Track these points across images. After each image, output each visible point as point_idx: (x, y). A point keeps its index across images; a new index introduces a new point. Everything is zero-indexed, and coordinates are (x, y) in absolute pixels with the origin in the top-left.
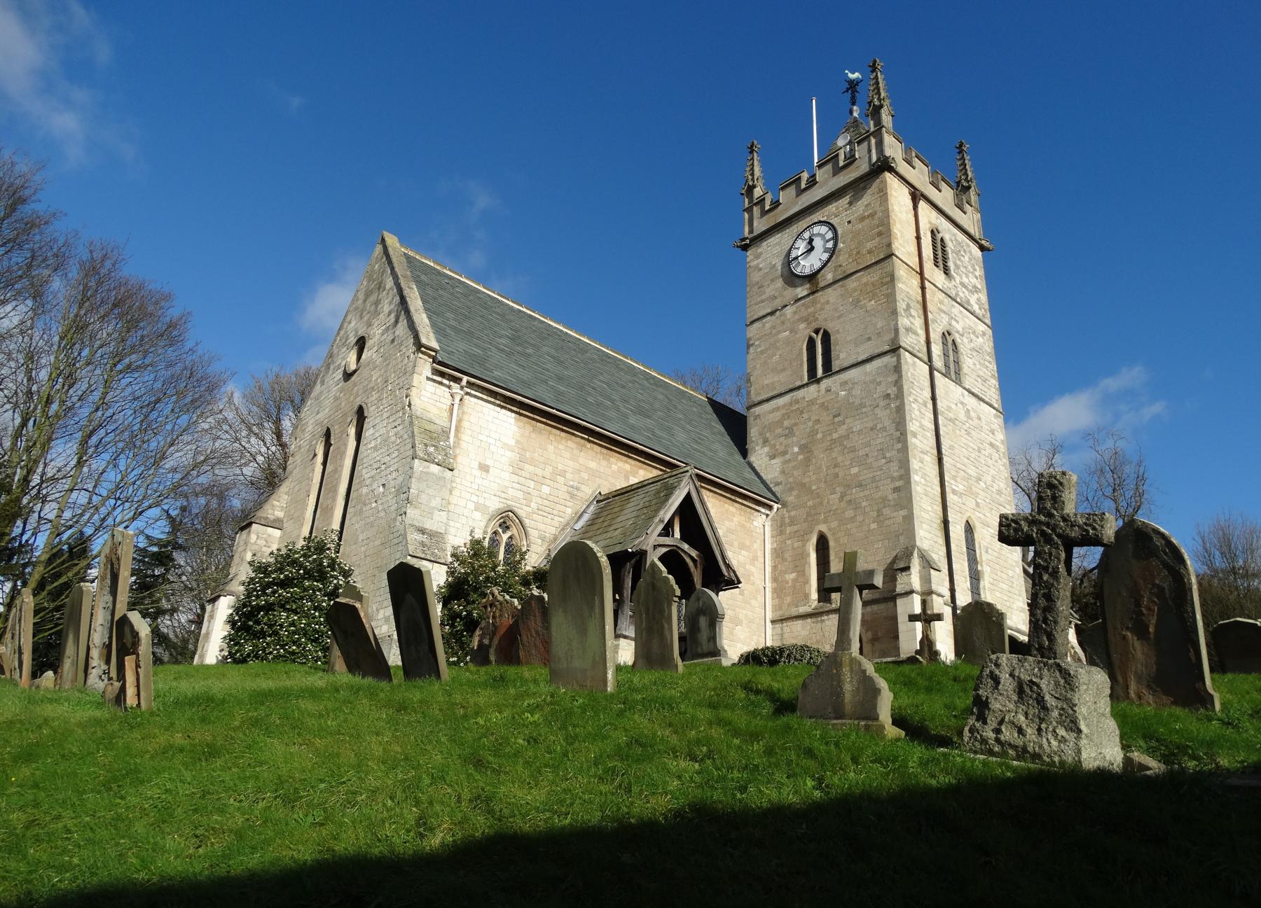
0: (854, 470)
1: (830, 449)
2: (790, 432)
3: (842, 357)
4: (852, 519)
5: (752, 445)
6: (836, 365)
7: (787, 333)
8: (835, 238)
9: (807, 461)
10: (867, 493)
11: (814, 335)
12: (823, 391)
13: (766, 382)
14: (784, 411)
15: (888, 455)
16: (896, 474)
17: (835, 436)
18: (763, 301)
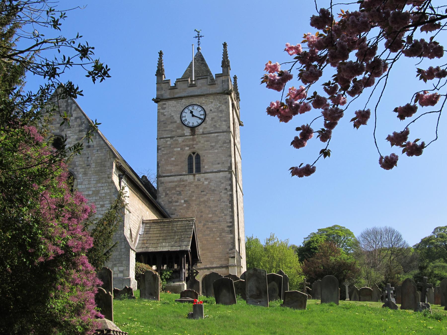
0: (210, 216)
1: (199, 205)
2: (180, 194)
3: (205, 166)
4: (209, 235)
5: (159, 194)
6: (202, 170)
7: (179, 149)
8: (205, 115)
9: (188, 208)
10: (216, 225)
11: (192, 155)
12: (196, 180)
13: (167, 168)
14: (176, 184)
15: (225, 212)
16: (229, 221)
17: (202, 200)
18: (165, 130)
